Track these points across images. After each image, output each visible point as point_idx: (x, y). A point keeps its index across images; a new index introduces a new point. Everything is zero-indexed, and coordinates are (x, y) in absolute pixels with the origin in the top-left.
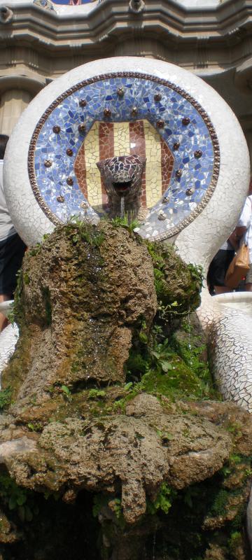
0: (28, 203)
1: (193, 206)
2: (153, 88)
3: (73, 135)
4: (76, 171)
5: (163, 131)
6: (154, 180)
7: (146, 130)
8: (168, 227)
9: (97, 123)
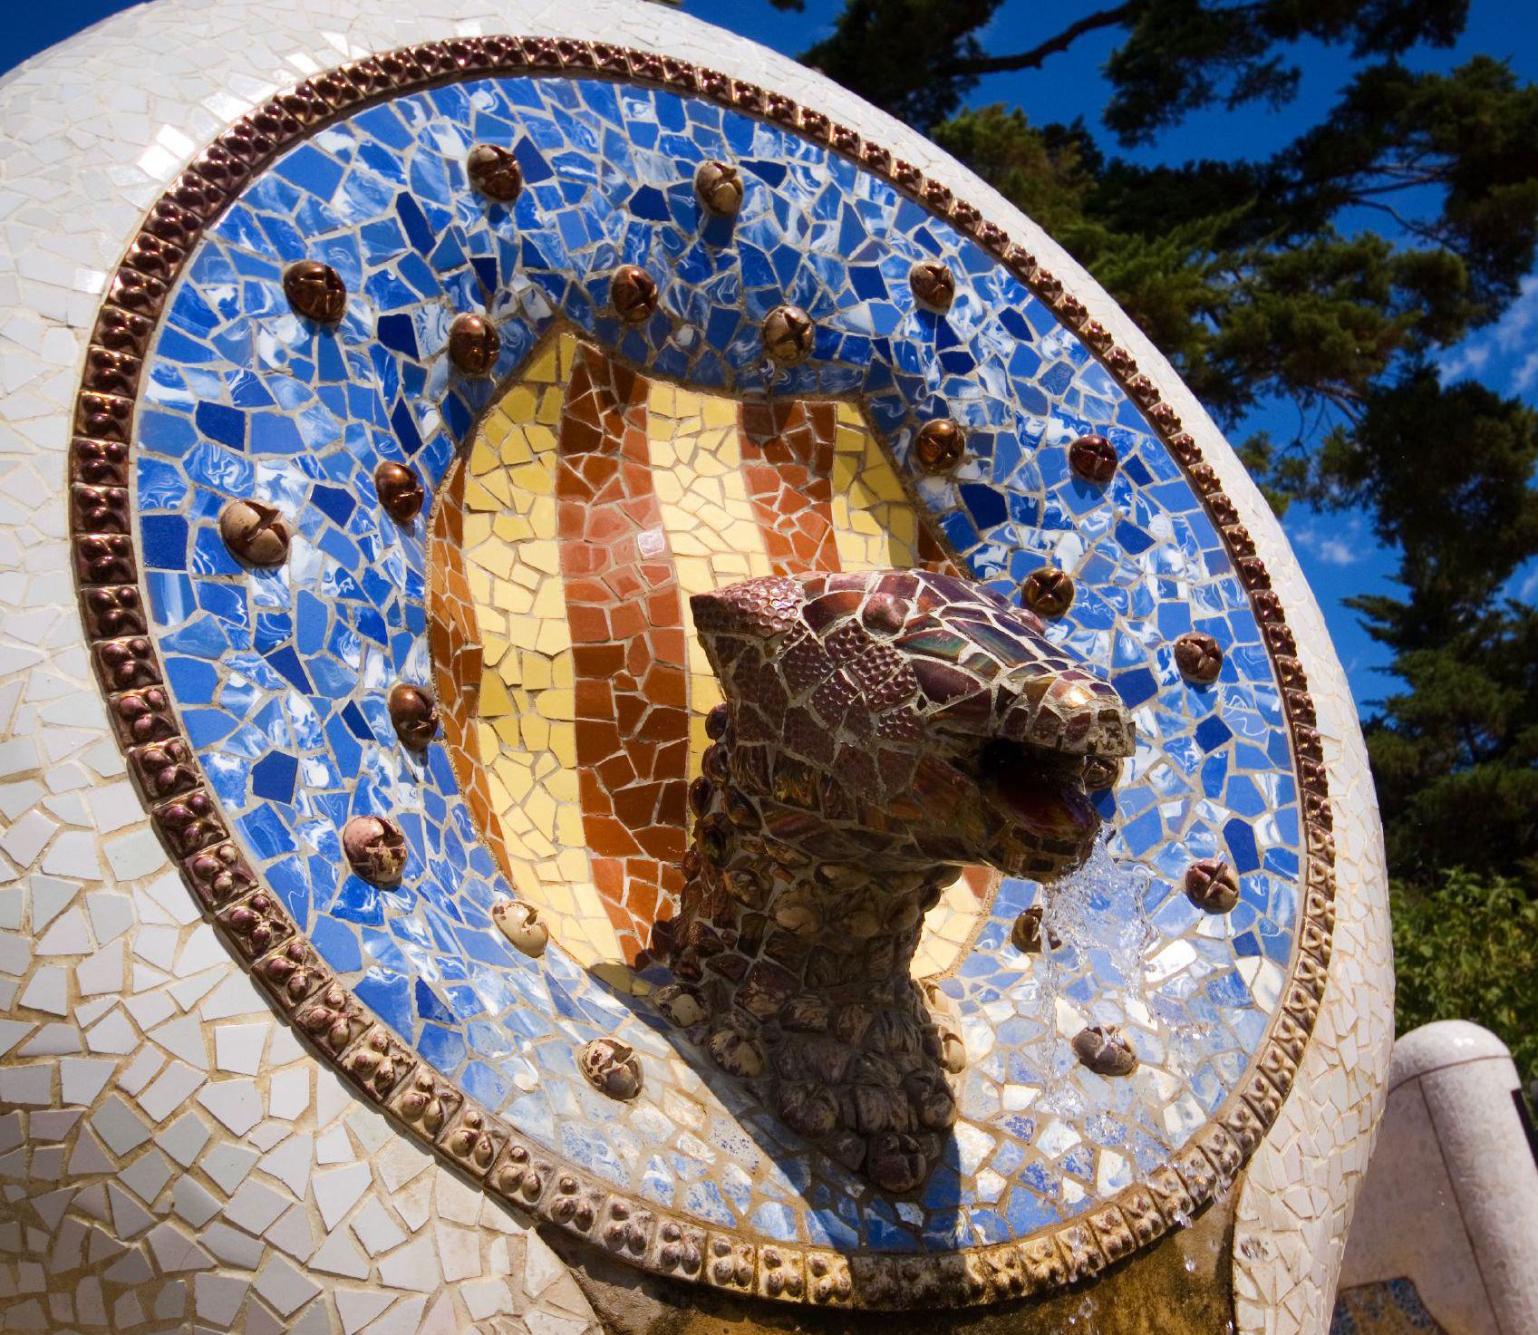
0: (73, 858)
2: (902, 224)
3: (415, 379)
7: (841, 471)
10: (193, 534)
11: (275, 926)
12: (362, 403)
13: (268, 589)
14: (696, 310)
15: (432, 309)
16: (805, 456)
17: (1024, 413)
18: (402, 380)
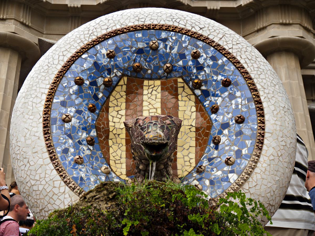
0: (40, 162)
1: (233, 177)
3: (98, 89)
4: (98, 130)
5: (198, 92)
6: (186, 146)
7: (180, 90)
9: (126, 79)
10: (58, 120)
11: (62, 170)
12: (87, 96)
13: (68, 126)
15: (100, 79)
16: (172, 88)
17: (213, 75)
18: (94, 90)
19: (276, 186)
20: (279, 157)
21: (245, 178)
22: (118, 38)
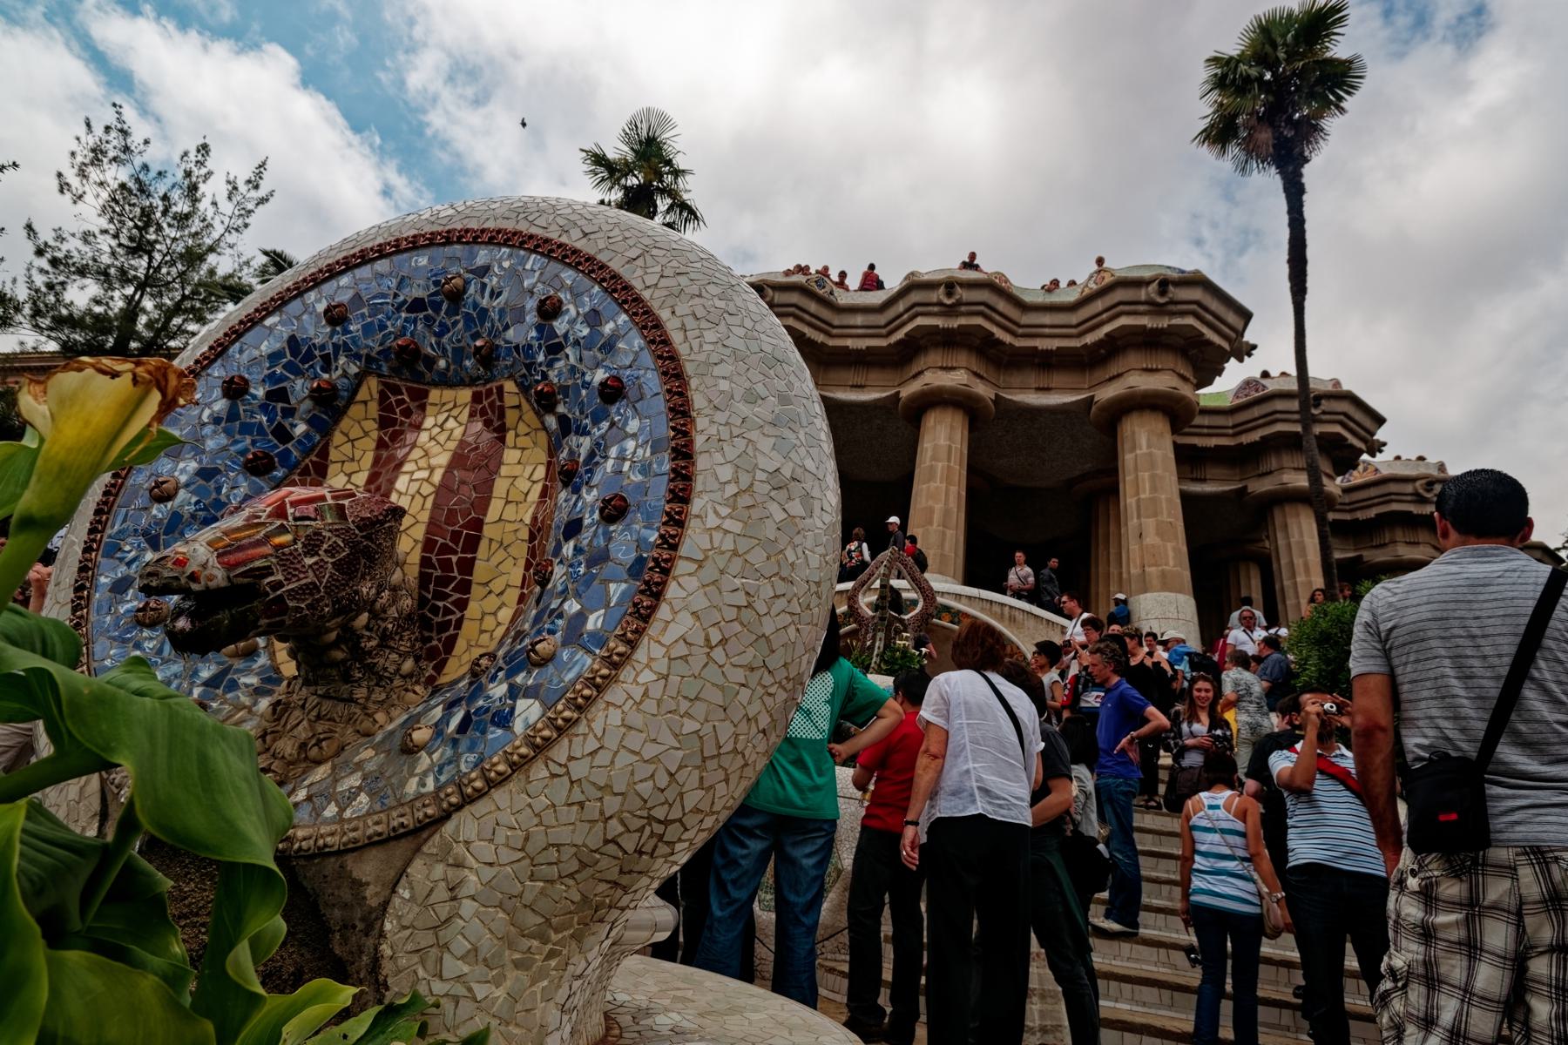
6: (497, 586)
7: (511, 416)
8: (412, 787)
9: (373, 384)
14: (444, 350)
15: (299, 382)
19: (680, 754)
20: (712, 648)
21: (560, 722)
22: (365, 272)
